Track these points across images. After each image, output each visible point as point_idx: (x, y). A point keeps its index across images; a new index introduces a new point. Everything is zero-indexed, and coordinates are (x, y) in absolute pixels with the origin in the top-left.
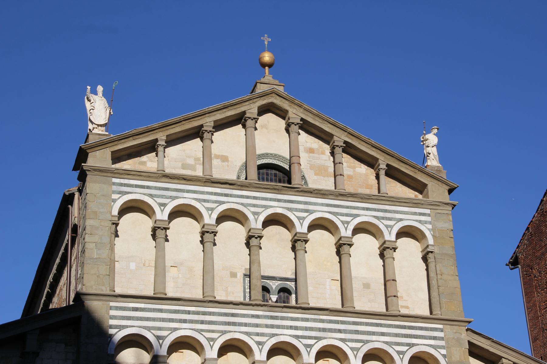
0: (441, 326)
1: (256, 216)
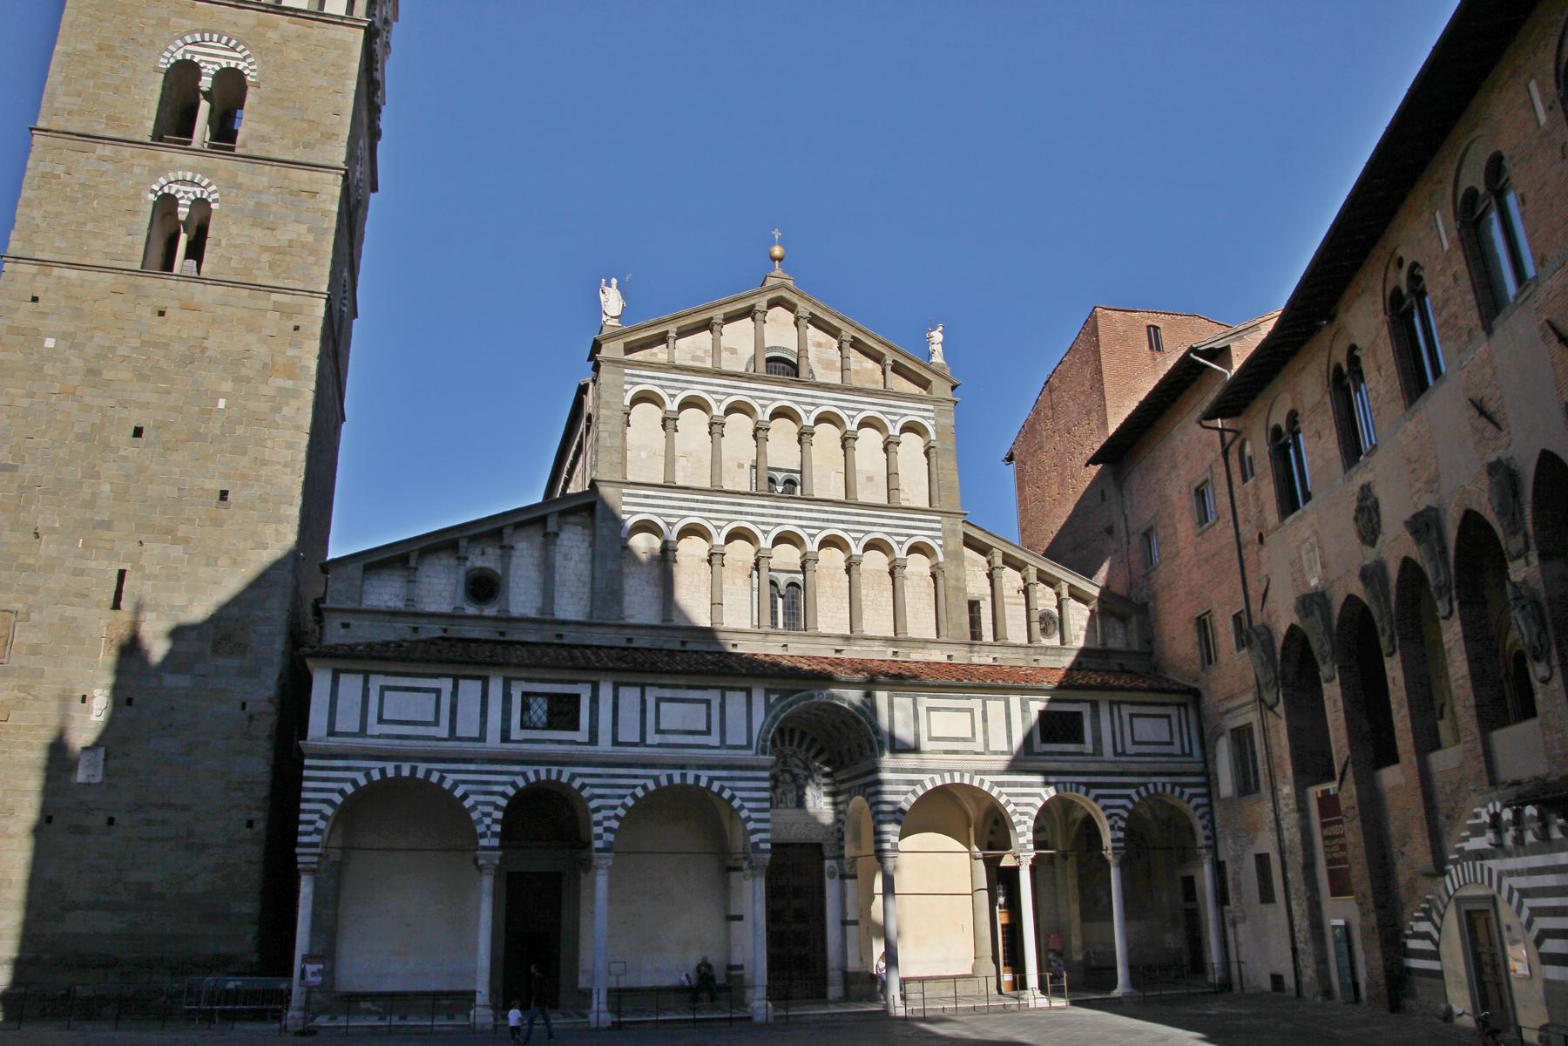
0: (939, 518)
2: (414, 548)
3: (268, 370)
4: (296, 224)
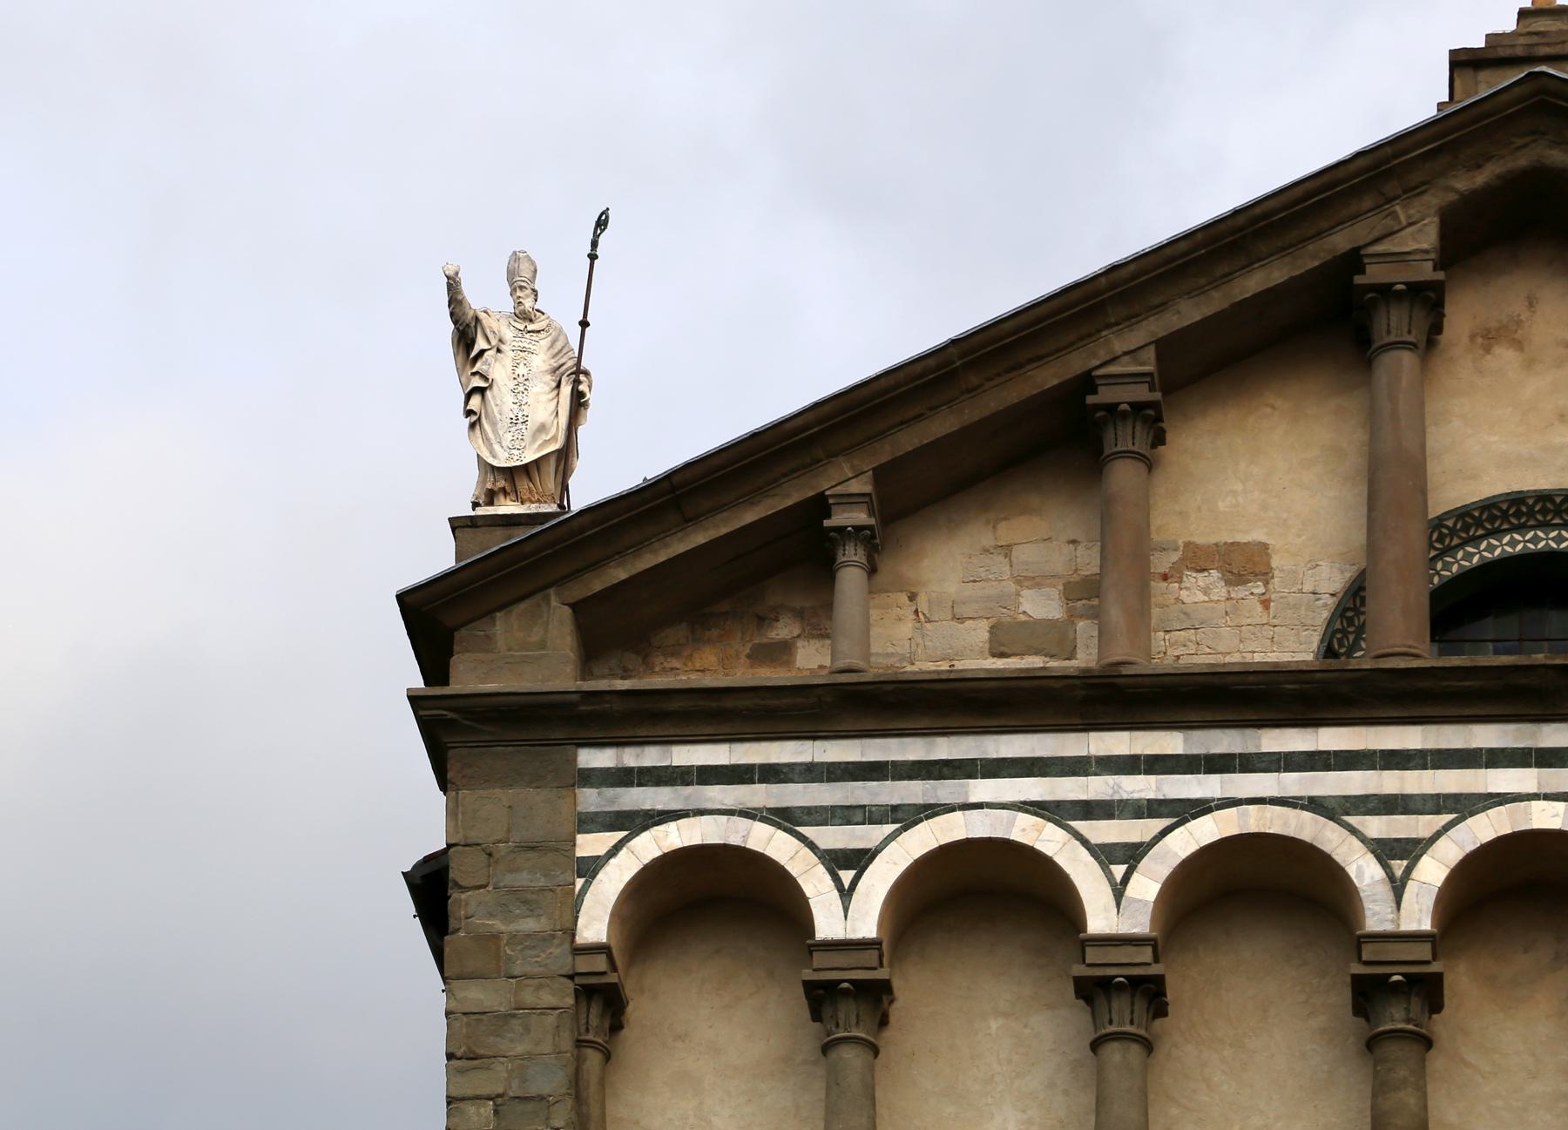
1: (1399, 866)
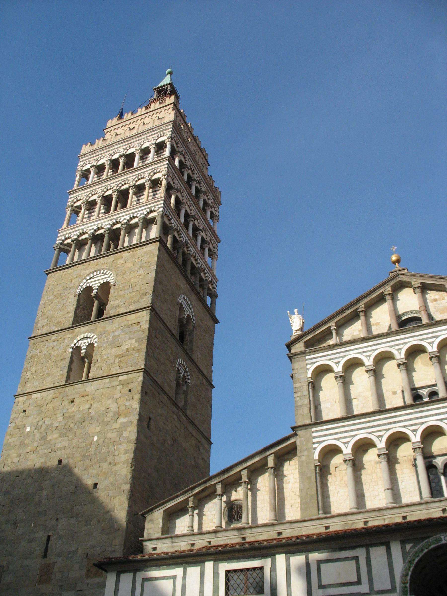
1: (399, 351)
2: (191, 495)
3: (118, 414)
4: (130, 341)
